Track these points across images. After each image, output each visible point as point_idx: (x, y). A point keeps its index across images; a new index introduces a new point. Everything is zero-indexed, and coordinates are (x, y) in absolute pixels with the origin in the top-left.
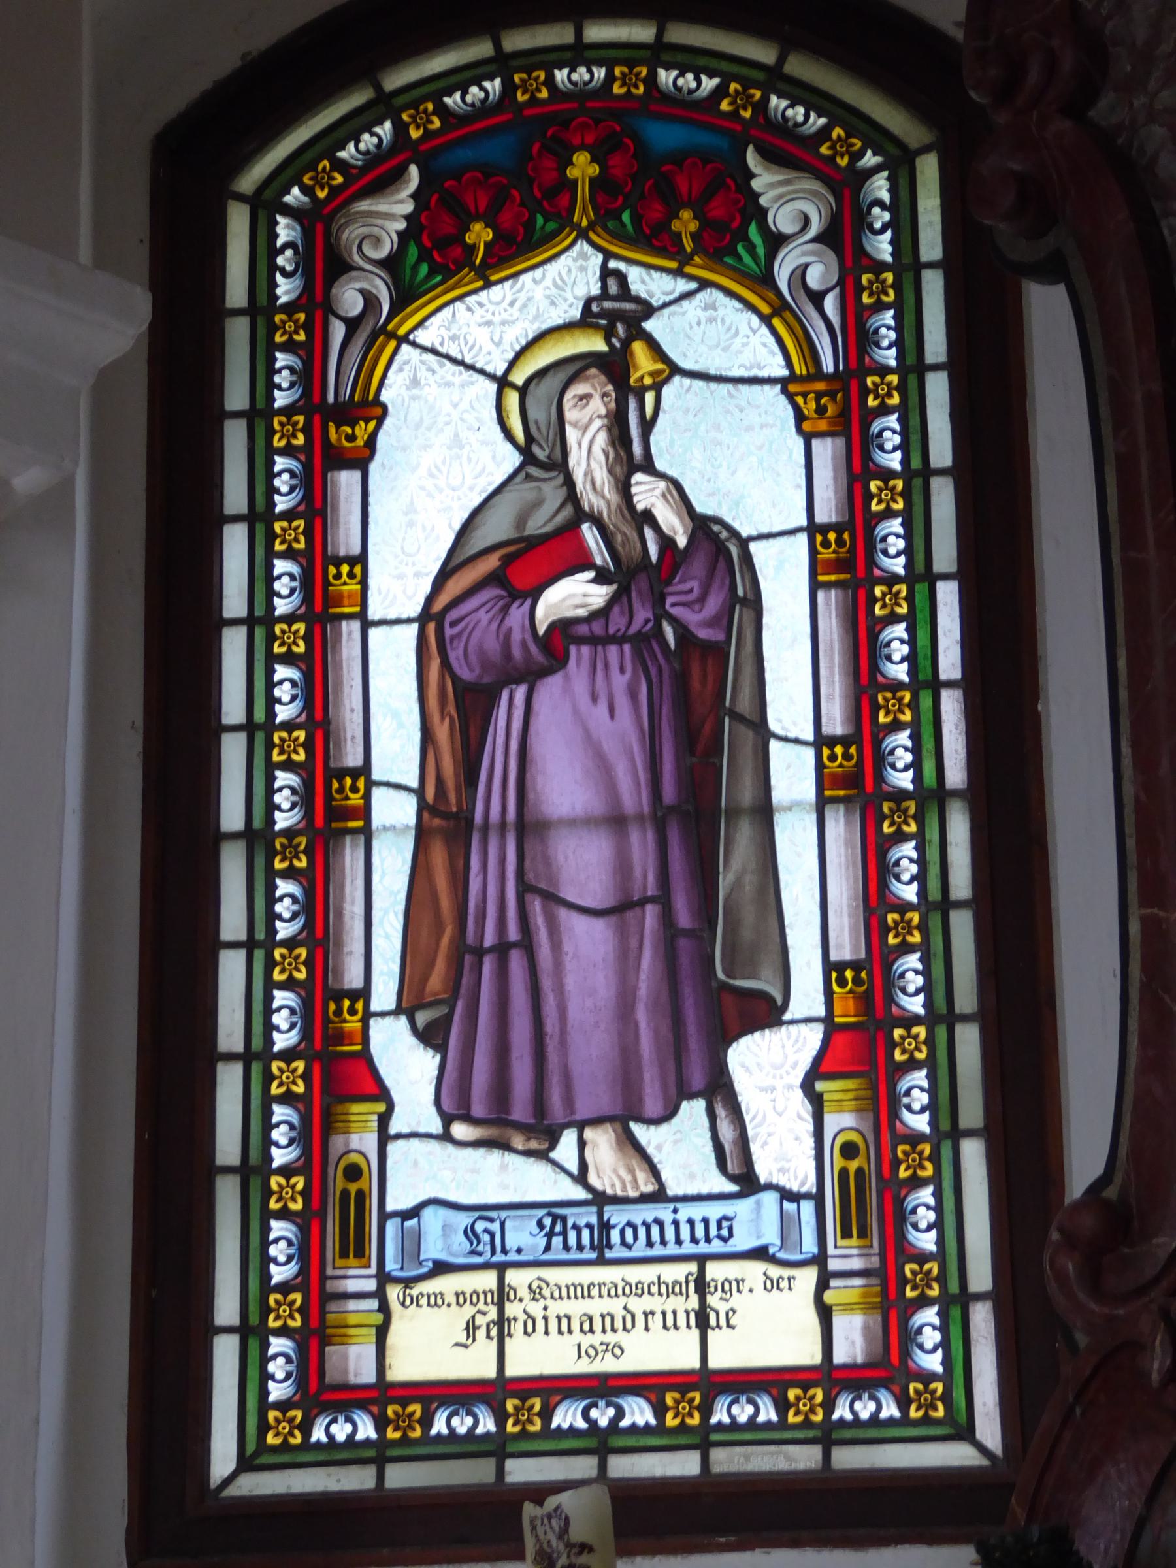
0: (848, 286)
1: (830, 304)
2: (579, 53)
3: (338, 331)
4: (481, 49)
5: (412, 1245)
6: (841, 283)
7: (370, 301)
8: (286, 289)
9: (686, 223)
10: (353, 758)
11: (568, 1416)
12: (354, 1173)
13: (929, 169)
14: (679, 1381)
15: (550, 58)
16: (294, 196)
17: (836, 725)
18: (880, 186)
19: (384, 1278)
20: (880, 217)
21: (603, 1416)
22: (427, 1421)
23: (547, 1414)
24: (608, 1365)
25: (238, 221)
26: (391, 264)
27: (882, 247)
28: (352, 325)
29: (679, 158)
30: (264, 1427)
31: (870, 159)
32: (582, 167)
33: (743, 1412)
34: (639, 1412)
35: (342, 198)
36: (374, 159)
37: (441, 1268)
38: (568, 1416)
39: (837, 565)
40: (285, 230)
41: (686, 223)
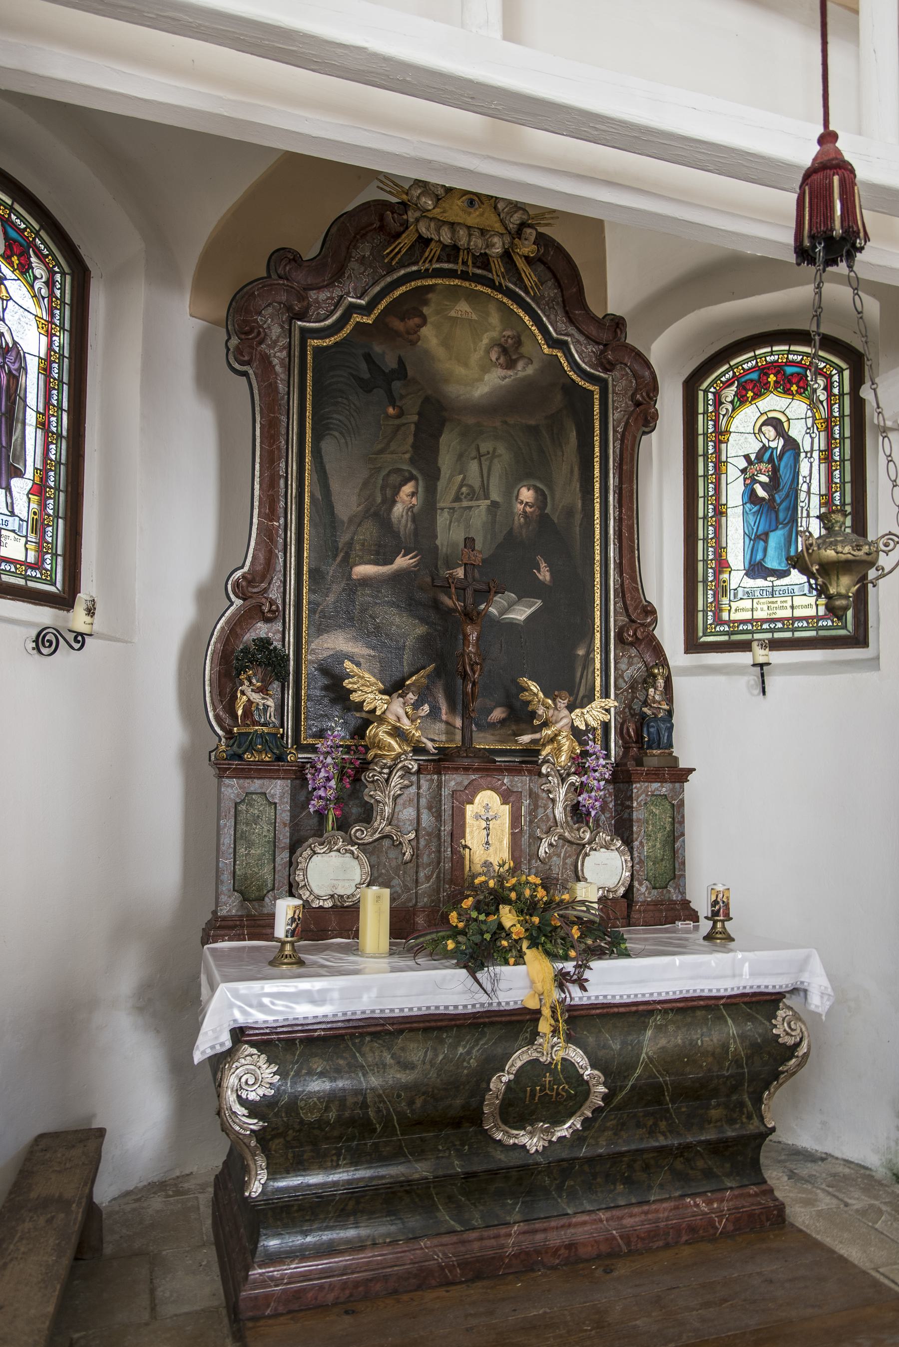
0: (828, 399)
1: (825, 404)
2: (772, 353)
3: (721, 417)
4: (752, 354)
5: (735, 595)
6: (827, 399)
7: (727, 409)
8: (711, 409)
9: (794, 388)
10: (724, 502)
11: (765, 626)
12: (724, 582)
13: (846, 373)
14: (788, 619)
15: (765, 355)
16: (712, 390)
17: (823, 492)
18: (836, 378)
19: (730, 600)
20: (836, 384)
21: (772, 626)
22: (738, 627)
23: (761, 626)
24: (774, 616)
25: (701, 394)
26: (732, 402)
27: (836, 391)
28: (724, 416)
29: (792, 375)
30: (707, 628)
31: (834, 372)
32: (772, 378)
33: (800, 625)
34: (779, 625)
35: (722, 389)
36: (728, 380)
37: (741, 599)
38: (765, 626)
39: (825, 459)
40: (710, 396)
41: (794, 388)
